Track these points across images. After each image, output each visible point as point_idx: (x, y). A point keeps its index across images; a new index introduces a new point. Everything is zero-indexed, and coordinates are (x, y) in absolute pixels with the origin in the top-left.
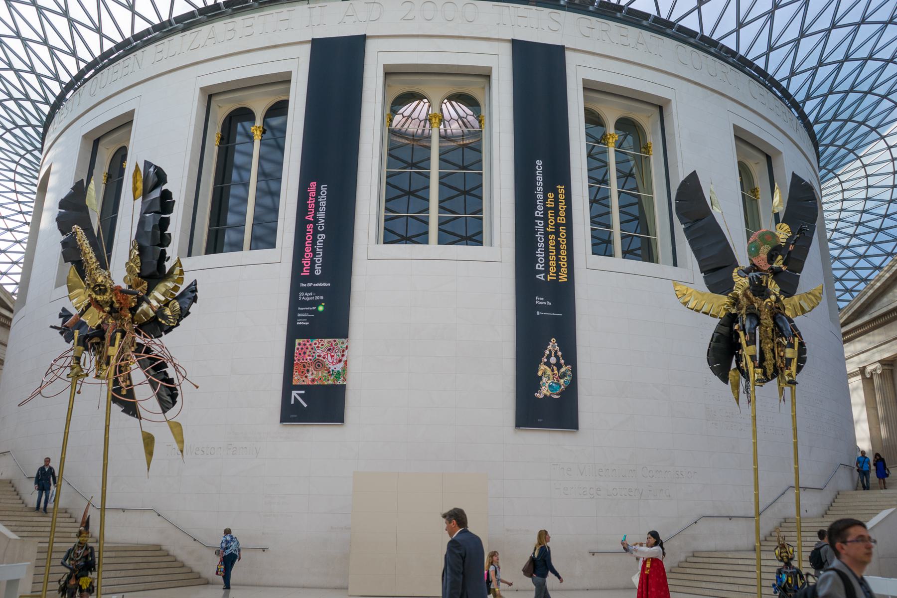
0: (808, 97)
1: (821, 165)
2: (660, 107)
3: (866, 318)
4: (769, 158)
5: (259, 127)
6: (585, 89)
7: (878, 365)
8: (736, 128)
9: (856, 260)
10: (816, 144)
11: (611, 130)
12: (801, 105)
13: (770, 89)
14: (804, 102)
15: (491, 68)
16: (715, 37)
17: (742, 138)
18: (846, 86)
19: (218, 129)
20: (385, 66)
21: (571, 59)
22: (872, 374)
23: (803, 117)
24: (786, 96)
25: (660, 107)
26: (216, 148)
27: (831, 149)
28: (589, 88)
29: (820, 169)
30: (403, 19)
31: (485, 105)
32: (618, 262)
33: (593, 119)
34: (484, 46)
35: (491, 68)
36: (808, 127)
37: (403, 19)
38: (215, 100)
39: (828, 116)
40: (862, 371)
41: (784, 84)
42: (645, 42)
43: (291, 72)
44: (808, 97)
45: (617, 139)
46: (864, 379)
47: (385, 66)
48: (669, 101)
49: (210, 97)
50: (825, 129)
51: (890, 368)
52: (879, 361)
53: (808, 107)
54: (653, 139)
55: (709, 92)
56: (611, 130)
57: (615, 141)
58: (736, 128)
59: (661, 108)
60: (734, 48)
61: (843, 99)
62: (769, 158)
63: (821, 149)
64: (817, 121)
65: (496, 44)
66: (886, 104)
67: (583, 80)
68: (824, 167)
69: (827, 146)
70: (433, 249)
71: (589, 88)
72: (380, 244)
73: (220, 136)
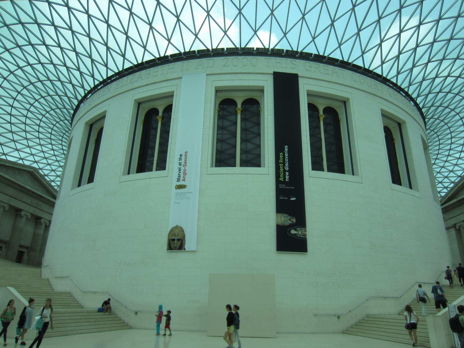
0: (418, 96)
1: (427, 128)
2: (345, 102)
3: (455, 200)
4: (399, 125)
5: (161, 117)
6: (308, 95)
8: (382, 110)
9: (65, 26)
10: (424, 118)
11: (321, 113)
12: (415, 99)
13: (399, 92)
14: (417, 98)
15: (264, 87)
16: (371, 69)
17: (385, 115)
18: (437, 90)
19: (143, 118)
20: (215, 87)
21: (301, 82)
23: (416, 105)
24: (407, 95)
25: (345, 102)
26: (142, 127)
27: (432, 120)
28: (310, 94)
29: (427, 130)
30: (224, 66)
31: (262, 104)
32: (326, 174)
33: (312, 108)
34: (261, 77)
35: (264, 87)
36: (420, 109)
37: (224, 66)
39: (429, 104)
41: (406, 90)
42: (336, 72)
43: (174, 91)
44: (418, 96)
45: (324, 117)
47: (215, 87)
48: (348, 99)
49: (139, 104)
50: (428, 110)
53: (418, 101)
54: (342, 117)
55: (368, 94)
56: (321, 113)
57: (323, 118)
58: (382, 110)
59: (345, 103)
60: (380, 74)
61: (436, 96)
62: (399, 125)
63: (426, 120)
64: (423, 107)
65: (266, 75)
66: (458, 98)
67: (307, 91)
68: (429, 129)
69: (430, 119)
70: (238, 169)
71: (310, 94)
72: (213, 167)
73: (143, 121)
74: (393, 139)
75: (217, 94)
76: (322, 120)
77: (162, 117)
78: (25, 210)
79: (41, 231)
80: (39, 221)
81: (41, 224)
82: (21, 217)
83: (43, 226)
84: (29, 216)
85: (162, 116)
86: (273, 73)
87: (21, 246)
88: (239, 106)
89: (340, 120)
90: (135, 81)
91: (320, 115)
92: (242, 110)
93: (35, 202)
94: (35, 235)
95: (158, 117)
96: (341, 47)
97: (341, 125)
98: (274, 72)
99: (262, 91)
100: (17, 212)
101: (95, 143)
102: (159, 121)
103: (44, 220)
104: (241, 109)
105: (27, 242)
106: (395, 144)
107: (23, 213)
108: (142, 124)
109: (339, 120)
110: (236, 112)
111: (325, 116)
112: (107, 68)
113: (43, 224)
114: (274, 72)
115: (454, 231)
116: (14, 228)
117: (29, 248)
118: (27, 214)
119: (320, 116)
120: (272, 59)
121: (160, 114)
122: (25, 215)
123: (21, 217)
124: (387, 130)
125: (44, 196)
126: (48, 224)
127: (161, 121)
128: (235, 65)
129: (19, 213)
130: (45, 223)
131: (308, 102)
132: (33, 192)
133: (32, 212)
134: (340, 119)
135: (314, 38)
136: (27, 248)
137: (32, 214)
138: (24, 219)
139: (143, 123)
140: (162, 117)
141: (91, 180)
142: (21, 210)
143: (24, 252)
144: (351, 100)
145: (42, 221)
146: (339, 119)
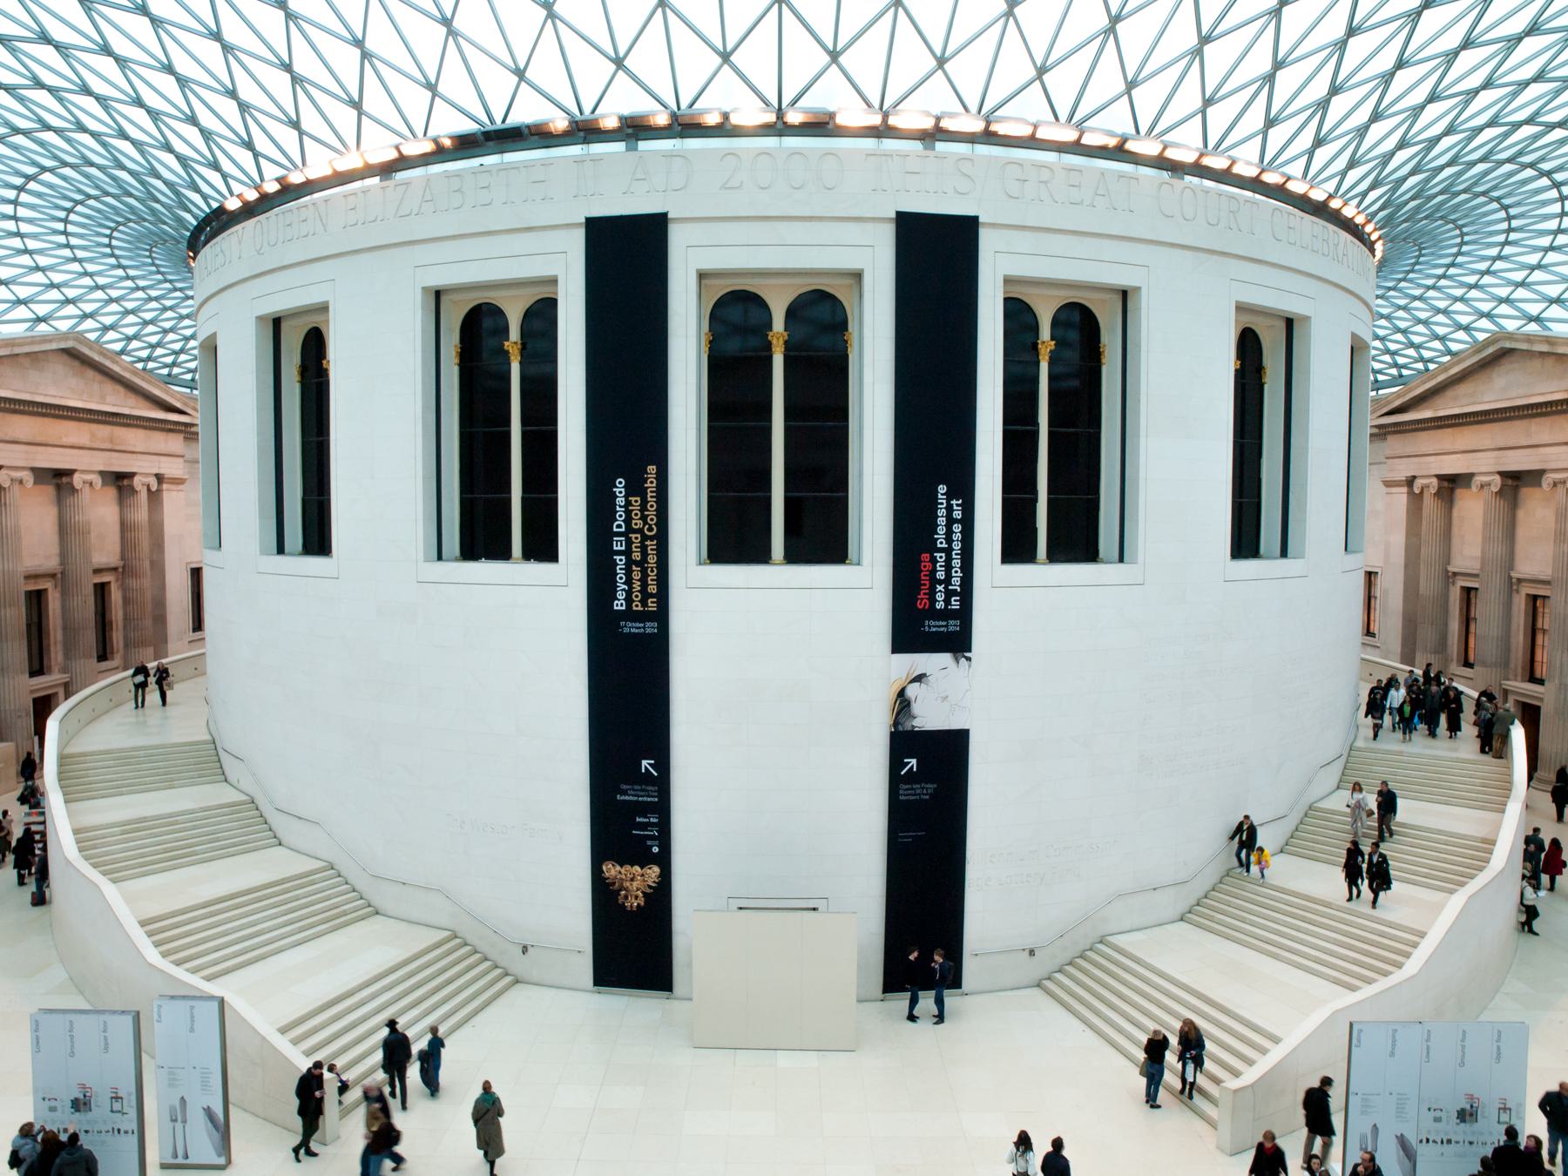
2: (1124, 295)
5: (515, 343)
7: (1435, 481)
21: (988, 243)
22: (1422, 492)
26: (456, 369)
30: (724, 187)
33: (1018, 314)
34: (852, 232)
37: (724, 187)
38: (443, 299)
40: (1410, 482)
45: (1053, 348)
46: (1411, 493)
47: (697, 270)
51: (1451, 486)
52: (1438, 476)
56: (1045, 333)
65: (869, 226)
73: (459, 350)
74: (1259, 369)
75: (703, 282)
76: (1047, 358)
77: (522, 344)
78: (79, 468)
79: (140, 512)
81: (133, 491)
83: (143, 495)
85: (520, 342)
86: (893, 215)
87: (97, 571)
88: (778, 324)
89: (1103, 351)
90: (415, 212)
91: (1039, 341)
92: (786, 338)
93: (103, 431)
94: (125, 527)
95: (506, 343)
96: (1133, 92)
97: (1104, 369)
98: (898, 213)
99: (857, 276)
100: (59, 479)
101: (298, 382)
102: (512, 358)
103: (140, 478)
104: (786, 334)
105: (106, 551)
106: (1266, 387)
107: (77, 480)
108: (457, 361)
109: (1101, 350)
110: (770, 344)
111: (1055, 345)
112: (301, 133)
114: (898, 213)
115: (1406, 495)
117: (121, 570)
119: (1040, 346)
120: (889, 159)
121: (514, 334)
122: (84, 482)
124: (1248, 345)
125: (126, 411)
126: (154, 488)
127: (519, 358)
128: (762, 186)
129: (64, 480)
130: (145, 488)
131: (1007, 296)
133: (102, 468)
134: (1105, 346)
135: (1042, 71)
136: (115, 569)
137: (102, 473)
139: (458, 358)
140: (519, 346)
141: (318, 540)
142: (69, 473)
143: (109, 583)
144: (1144, 292)
146: (1101, 345)
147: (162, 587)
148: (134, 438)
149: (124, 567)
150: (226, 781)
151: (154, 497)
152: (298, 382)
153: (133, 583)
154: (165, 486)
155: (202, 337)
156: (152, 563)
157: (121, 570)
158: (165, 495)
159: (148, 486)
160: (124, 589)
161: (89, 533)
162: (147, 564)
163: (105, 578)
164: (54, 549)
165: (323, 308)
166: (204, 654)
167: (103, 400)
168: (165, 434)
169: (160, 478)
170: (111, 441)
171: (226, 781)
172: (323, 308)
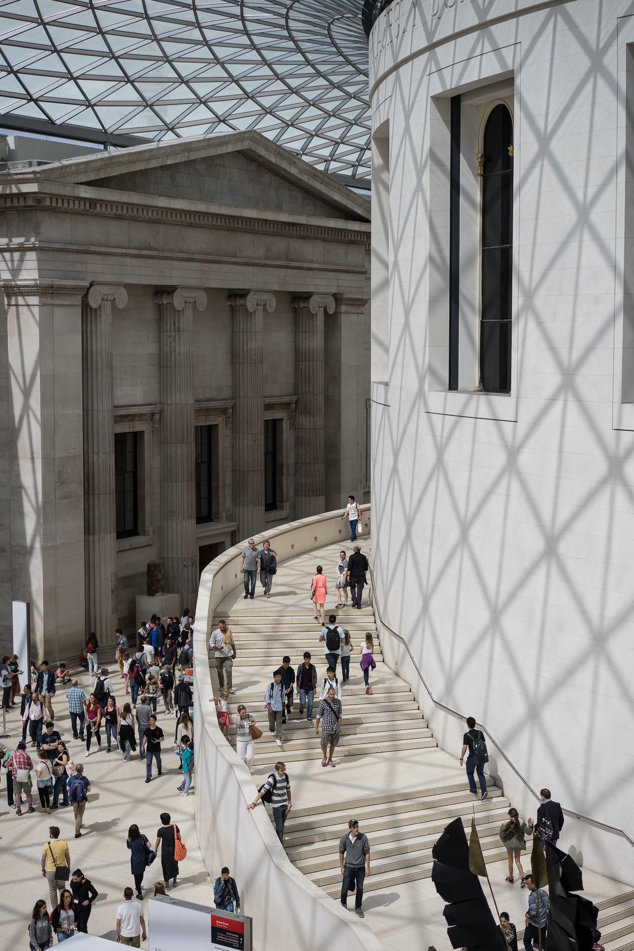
79: (316, 342)
80: (302, 305)
82: (249, 315)
84: (272, 302)
87: (269, 407)
93: (279, 245)
94: (299, 356)
107: (250, 303)
113: (317, 314)
116: (235, 357)
117: (293, 406)
118: (265, 297)
123: (249, 315)
125: (303, 220)
126: (331, 311)
129: (239, 302)
132: (266, 221)
133: (276, 288)
136: (288, 405)
137: (276, 293)
138: (259, 318)
142: (241, 294)
143: (282, 420)
145: (314, 304)
147: (338, 427)
148: (310, 250)
149: (296, 403)
150: (383, 661)
151: (331, 320)
152: (480, 175)
153: (305, 421)
154: (343, 308)
155: (375, 124)
156: (327, 398)
157: (293, 406)
158: (343, 318)
159: (325, 308)
160: (294, 425)
161: (261, 362)
162: (321, 399)
163: (278, 415)
164: (227, 381)
165: (507, 81)
166: (369, 509)
167: (279, 208)
168: (345, 246)
169: (338, 298)
170: (288, 259)
171: (383, 661)
172: (507, 81)
